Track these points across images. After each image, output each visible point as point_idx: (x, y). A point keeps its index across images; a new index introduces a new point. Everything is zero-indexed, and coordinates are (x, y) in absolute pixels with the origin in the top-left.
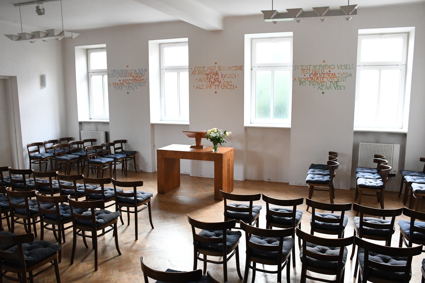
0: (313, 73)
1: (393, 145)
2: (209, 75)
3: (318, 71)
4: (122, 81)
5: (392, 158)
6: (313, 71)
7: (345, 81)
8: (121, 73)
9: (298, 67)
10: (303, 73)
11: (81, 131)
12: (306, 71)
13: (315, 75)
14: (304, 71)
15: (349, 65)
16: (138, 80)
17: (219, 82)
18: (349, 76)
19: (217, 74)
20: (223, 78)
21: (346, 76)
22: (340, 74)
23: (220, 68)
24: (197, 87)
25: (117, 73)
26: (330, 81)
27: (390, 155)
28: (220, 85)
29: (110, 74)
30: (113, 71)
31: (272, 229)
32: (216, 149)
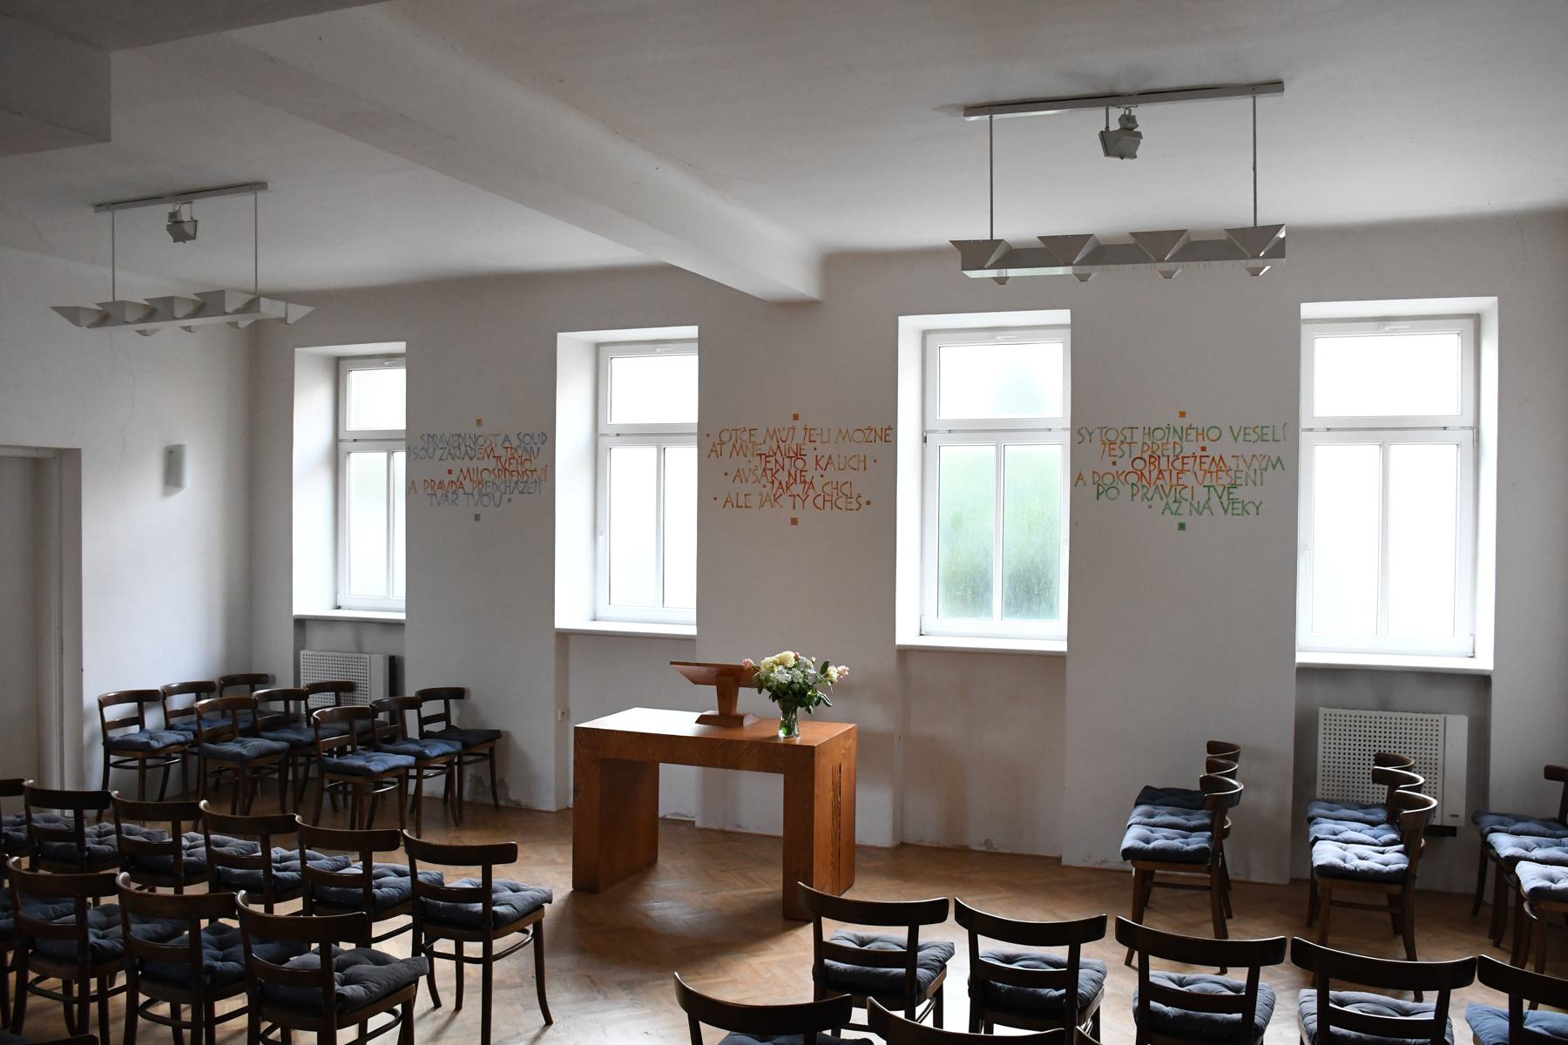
0: (1146, 456)
1: (1441, 717)
2: (772, 459)
3: (1161, 448)
4: (456, 473)
5: (1440, 767)
6: (1143, 448)
7: (1258, 483)
8: (456, 444)
9: (1090, 434)
10: (1110, 456)
11: (302, 652)
12: (1120, 447)
13: (1153, 463)
14: (1112, 446)
15: (1271, 427)
17: (807, 485)
18: (1274, 467)
19: (799, 455)
20: (820, 471)
21: (1264, 466)
22: (1241, 459)
23: (810, 435)
24: (727, 501)
25: (441, 446)
26: (1207, 483)
27: (1434, 757)
28: (812, 493)
29: (416, 448)
30: (425, 438)
31: (992, 1033)
32: (790, 731)
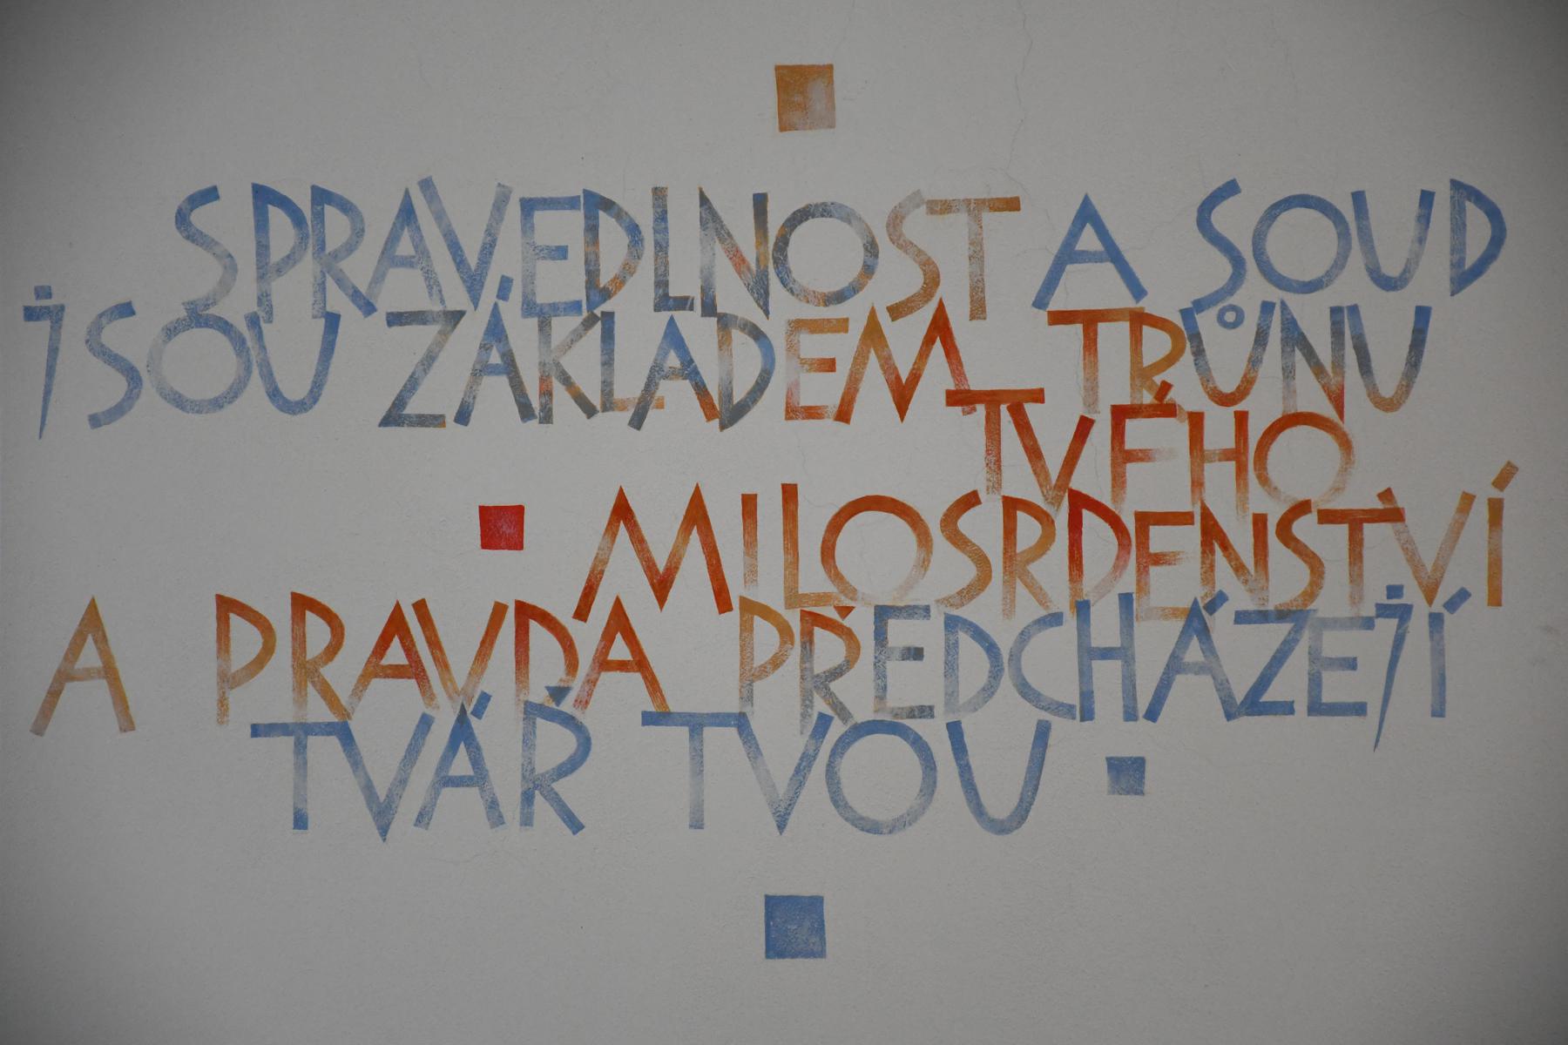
16: (1160, 539)
